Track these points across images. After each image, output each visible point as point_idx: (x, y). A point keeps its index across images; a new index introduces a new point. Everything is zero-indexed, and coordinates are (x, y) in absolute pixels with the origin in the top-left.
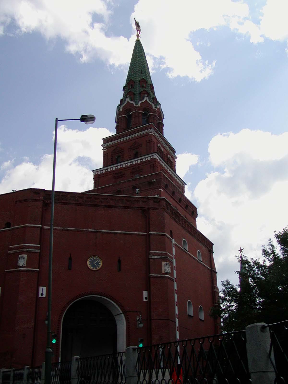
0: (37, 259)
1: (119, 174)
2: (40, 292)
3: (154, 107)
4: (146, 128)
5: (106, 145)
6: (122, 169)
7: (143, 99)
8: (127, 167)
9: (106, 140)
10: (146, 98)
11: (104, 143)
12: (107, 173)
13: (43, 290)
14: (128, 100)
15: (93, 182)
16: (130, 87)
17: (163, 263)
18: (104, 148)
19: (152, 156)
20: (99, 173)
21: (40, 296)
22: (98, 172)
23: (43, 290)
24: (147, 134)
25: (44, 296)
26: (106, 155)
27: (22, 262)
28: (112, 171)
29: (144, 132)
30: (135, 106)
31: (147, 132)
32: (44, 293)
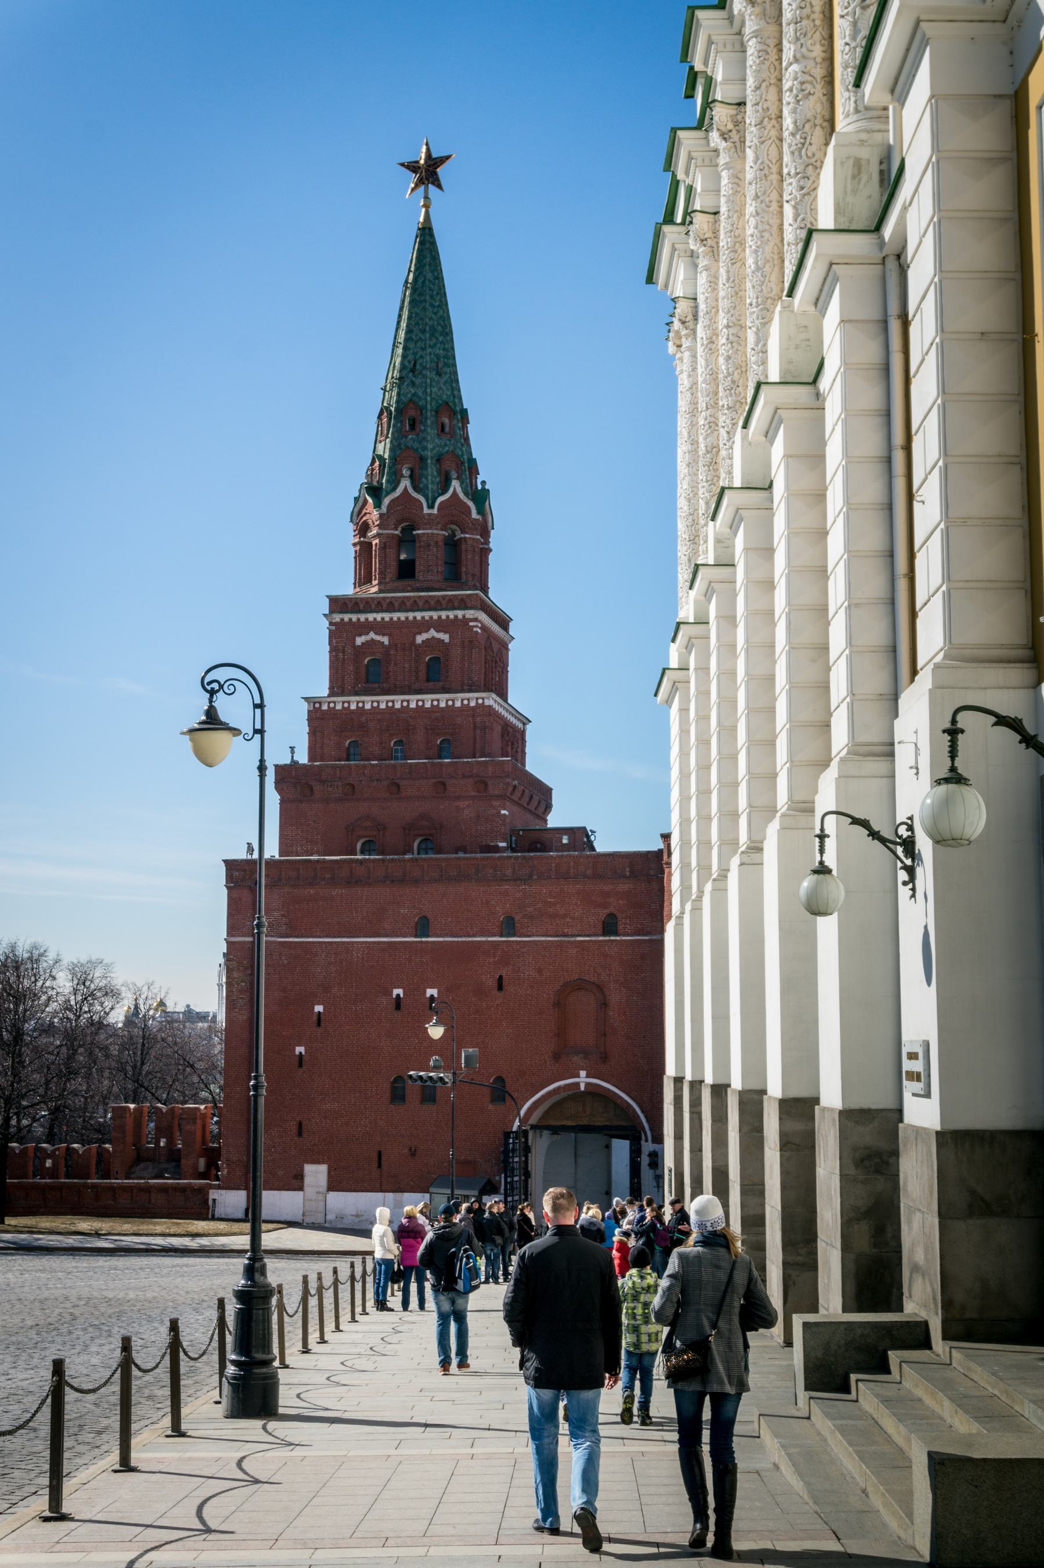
3: (474, 515)
4: (463, 604)
5: (337, 618)
9: (338, 604)
10: (455, 484)
11: (332, 611)
14: (405, 483)
15: (307, 729)
18: (331, 624)
19: (483, 699)
20: (325, 707)
22: (320, 703)
24: (465, 621)
29: (460, 614)
30: (426, 511)
31: (467, 616)
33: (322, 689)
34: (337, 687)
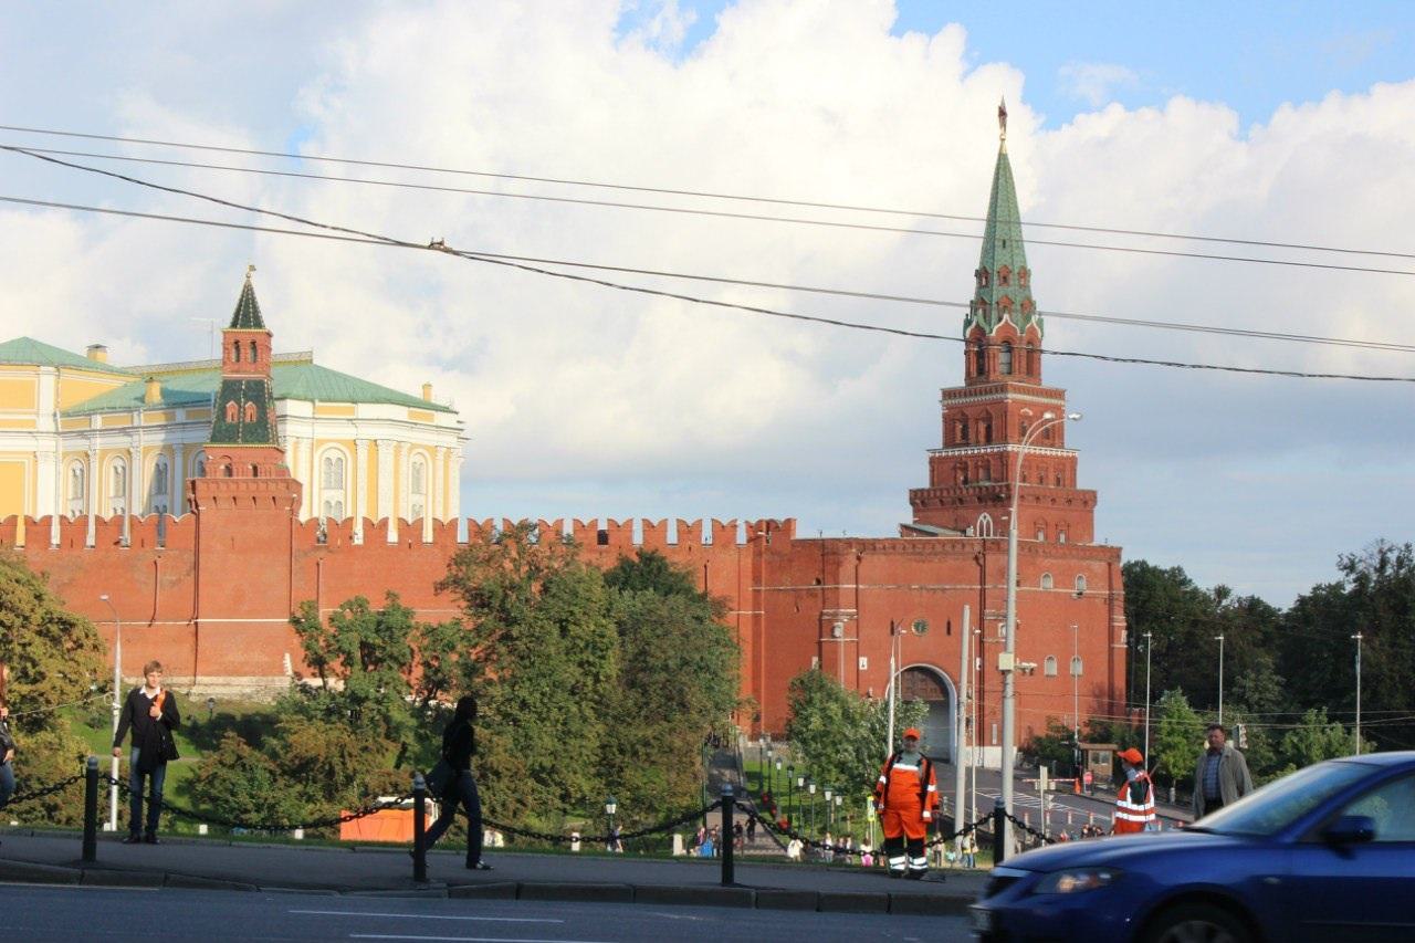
0: (857, 625)
1: (961, 464)
2: (861, 665)
5: (946, 402)
6: (966, 456)
7: (1000, 319)
8: (973, 456)
9: (948, 394)
10: (1006, 317)
12: (947, 457)
13: (863, 661)
16: (984, 283)
17: (1001, 624)
21: (861, 668)
23: (863, 661)
25: (866, 668)
26: (949, 421)
27: (838, 632)
28: (953, 457)
32: (865, 663)
33: (939, 443)
34: (949, 442)
